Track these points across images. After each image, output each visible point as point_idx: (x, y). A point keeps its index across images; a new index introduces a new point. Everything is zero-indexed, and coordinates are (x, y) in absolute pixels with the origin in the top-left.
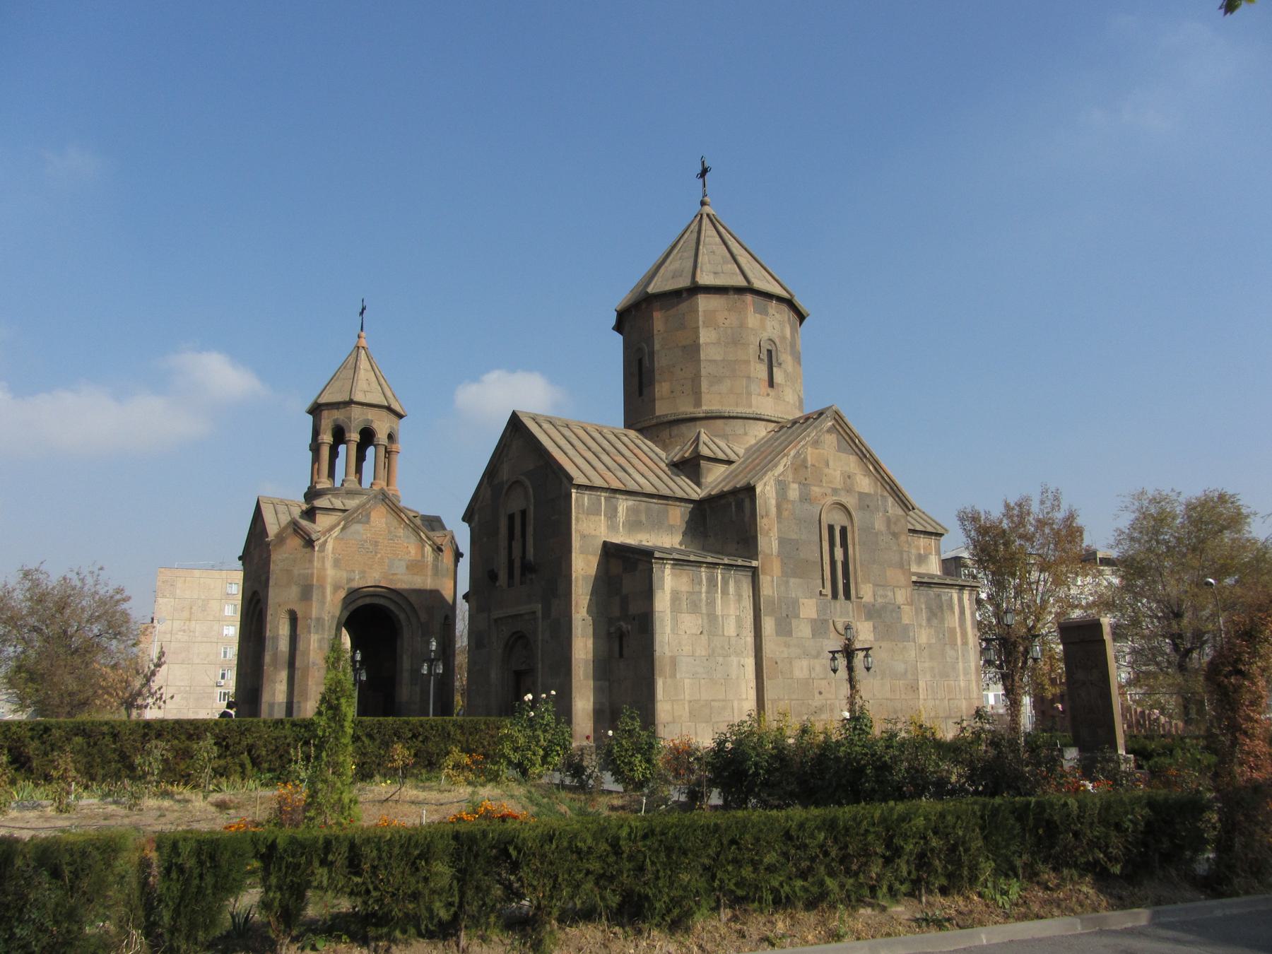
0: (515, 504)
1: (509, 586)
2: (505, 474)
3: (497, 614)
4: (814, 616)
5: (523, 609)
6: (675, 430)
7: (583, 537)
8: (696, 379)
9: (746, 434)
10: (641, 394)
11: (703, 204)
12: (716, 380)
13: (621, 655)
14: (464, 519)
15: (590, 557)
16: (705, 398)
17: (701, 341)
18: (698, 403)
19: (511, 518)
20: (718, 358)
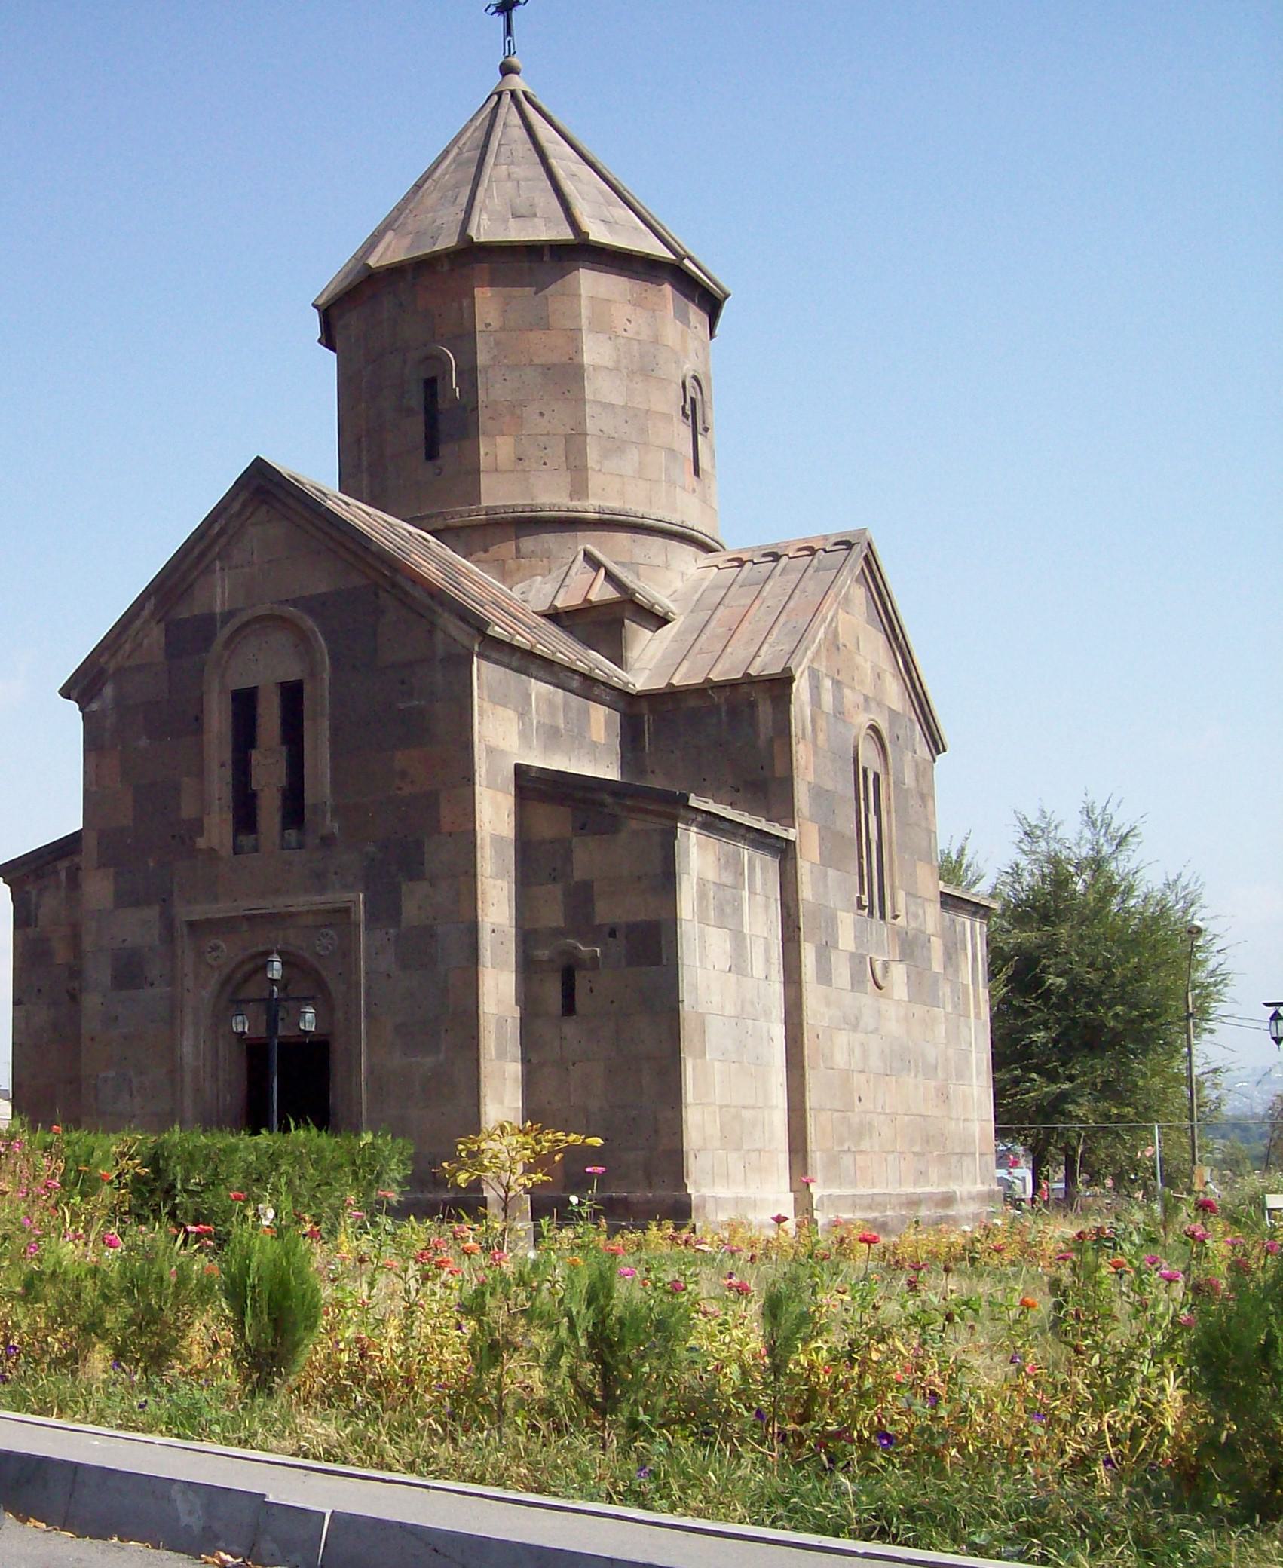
0: (266, 666)
1: (237, 850)
2: (219, 593)
3: (201, 911)
4: (852, 948)
5: (300, 902)
6: (528, 543)
7: (491, 751)
8: (575, 442)
9: (667, 567)
10: (432, 454)
11: (507, 69)
12: (615, 446)
13: (569, 1007)
14: (81, 687)
15: (500, 796)
16: (595, 481)
17: (587, 359)
18: (579, 489)
19: (245, 702)
20: (617, 400)
